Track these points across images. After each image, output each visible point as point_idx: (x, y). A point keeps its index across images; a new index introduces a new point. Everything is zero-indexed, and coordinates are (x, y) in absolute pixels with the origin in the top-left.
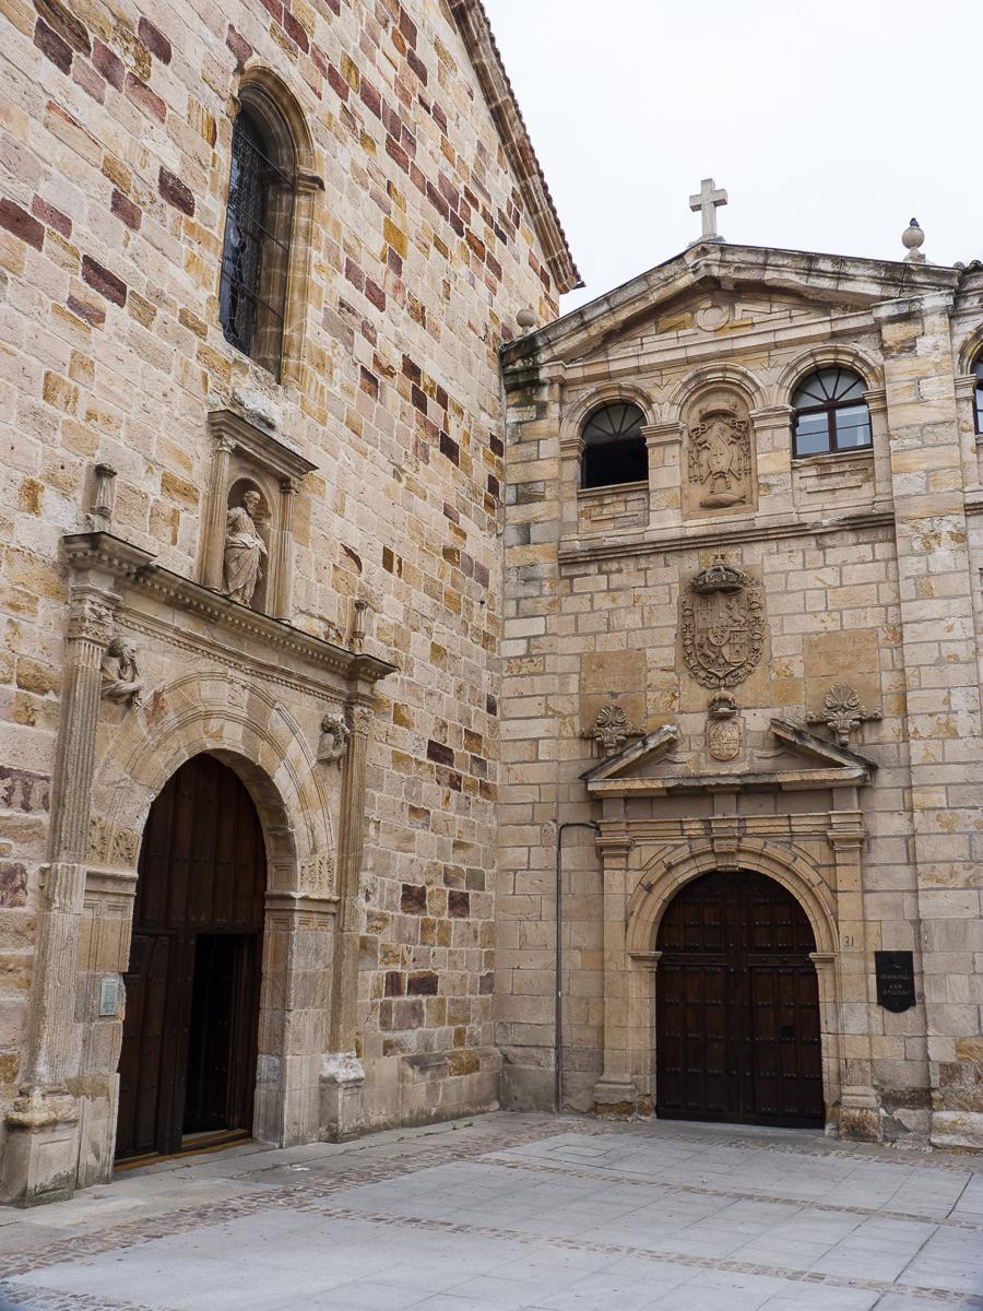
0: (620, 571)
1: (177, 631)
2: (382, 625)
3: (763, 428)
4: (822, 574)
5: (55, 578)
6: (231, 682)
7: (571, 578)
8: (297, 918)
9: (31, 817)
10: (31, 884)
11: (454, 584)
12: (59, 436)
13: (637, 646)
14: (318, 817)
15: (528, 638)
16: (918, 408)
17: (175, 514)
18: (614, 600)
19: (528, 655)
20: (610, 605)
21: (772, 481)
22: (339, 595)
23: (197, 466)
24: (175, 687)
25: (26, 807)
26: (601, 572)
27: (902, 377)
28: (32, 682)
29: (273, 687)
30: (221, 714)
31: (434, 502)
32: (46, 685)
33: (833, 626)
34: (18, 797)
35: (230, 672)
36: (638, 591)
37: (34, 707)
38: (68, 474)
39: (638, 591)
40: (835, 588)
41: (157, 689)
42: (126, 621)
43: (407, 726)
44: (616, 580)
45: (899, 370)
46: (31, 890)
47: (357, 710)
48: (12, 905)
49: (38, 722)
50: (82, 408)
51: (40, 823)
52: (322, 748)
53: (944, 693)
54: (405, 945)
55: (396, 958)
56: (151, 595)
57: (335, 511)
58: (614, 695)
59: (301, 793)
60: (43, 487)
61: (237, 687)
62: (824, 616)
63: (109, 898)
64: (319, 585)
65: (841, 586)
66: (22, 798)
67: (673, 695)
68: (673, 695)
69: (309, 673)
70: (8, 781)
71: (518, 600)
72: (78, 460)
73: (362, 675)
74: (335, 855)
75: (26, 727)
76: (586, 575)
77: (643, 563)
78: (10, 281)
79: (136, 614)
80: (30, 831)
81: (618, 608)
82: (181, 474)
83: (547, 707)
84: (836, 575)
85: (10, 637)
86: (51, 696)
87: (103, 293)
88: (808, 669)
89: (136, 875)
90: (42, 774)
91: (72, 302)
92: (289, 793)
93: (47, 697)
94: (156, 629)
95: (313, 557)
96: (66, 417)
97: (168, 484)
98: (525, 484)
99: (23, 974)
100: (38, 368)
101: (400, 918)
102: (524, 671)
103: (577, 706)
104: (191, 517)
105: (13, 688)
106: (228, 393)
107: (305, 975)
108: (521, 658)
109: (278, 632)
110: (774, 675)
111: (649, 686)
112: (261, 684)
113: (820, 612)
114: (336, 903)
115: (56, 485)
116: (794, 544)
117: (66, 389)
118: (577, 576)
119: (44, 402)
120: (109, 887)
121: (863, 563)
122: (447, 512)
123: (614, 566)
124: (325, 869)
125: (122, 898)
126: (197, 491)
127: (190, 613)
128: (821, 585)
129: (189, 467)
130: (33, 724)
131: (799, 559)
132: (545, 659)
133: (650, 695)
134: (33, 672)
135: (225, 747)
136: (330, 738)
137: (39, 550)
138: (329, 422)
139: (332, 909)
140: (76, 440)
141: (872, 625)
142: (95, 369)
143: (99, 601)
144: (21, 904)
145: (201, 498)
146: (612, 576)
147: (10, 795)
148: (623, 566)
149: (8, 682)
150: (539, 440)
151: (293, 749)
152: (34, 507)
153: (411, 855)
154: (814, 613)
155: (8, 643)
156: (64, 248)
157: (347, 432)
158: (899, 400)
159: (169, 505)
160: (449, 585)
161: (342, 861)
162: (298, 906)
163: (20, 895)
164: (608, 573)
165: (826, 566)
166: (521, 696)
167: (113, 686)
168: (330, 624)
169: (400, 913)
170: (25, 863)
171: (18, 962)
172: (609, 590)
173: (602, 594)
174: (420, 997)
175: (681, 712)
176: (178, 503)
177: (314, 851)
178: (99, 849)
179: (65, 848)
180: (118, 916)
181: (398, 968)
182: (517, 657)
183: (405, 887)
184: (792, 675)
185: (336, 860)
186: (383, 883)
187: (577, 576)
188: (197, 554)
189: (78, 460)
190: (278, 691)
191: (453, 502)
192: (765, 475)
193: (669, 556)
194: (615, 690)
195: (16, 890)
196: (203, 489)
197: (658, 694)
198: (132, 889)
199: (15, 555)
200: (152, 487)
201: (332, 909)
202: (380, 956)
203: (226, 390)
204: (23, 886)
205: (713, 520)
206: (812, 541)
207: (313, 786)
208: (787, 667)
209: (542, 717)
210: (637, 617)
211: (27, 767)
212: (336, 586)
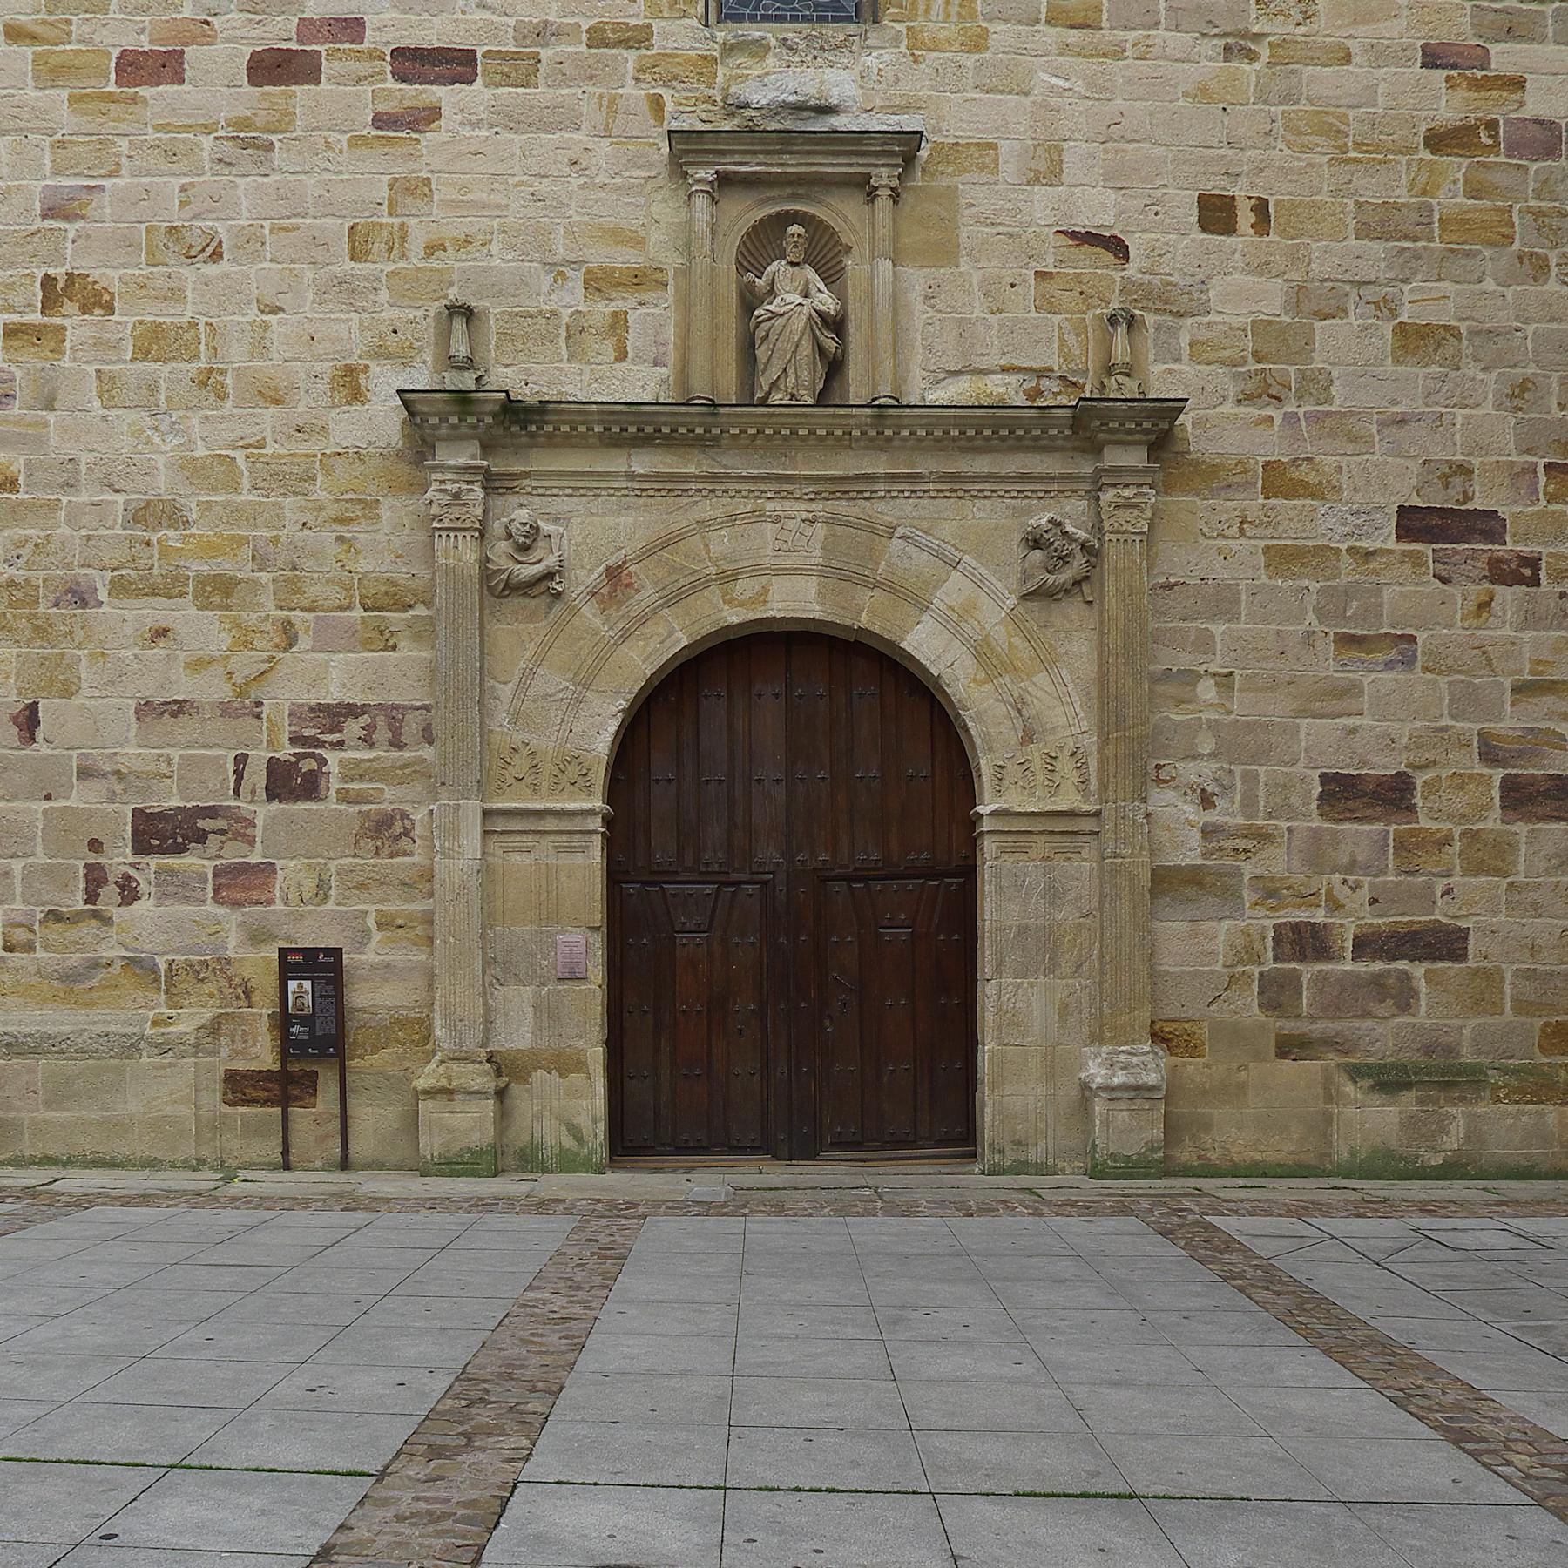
1: (631, 476)
2: (1203, 335)
5: (404, 469)
6: (778, 520)
8: (989, 846)
9: (406, 754)
10: (418, 831)
11: (1474, 192)
12: (384, 295)
14: (1040, 688)
17: (618, 323)
22: (1057, 319)
23: (655, 236)
24: (649, 552)
25: (397, 744)
28: (386, 600)
29: (879, 506)
30: (756, 571)
31: (1379, 54)
32: (410, 599)
34: (383, 734)
35: (770, 506)
37: (391, 629)
38: (406, 336)
41: (610, 563)
42: (536, 488)
43: (1313, 496)
46: (421, 838)
47: (1107, 496)
48: (392, 856)
49: (401, 645)
50: (416, 246)
51: (421, 760)
52: (1026, 577)
54: (1337, 877)
55: (1308, 899)
56: (556, 442)
57: (1035, 181)
59: (983, 653)
60: (367, 366)
61: (791, 524)
63: (551, 838)
64: (993, 319)
66: (390, 735)
69: (981, 464)
70: (365, 720)
72: (420, 313)
73: (1101, 436)
74: (1090, 741)
75: (385, 653)
78: (277, 144)
79: (527, 475)
80: (407, 771)
82: (625, 258)
85: (342, 556)
86: (420, 611)
87: (432, 83)
89: (597, 803)
90: (418, 704)
91: (379, 121)
92: (949, 659)
93: (412, 612)
94: (595, 484)
95: (976, 277)
96: (391, 267)
97: (597, 283)
99: (420, 930)
100: (335, 228)
101: (1316, 834)
104: (657, 311)
105: (358, 613)
106: (714, 103)
107: (1023, 930)
109: (851, 422)
112: (843, 506)
114: (1097, 814)
115: (389, 356)
117: (385, 234)
119: (353, 264)
120: (551, 824)
122: (1432, 58)
124: (1065, 766)
125: (577, 837)
126: (661, 270)
127: (659, 445)
129: (640, 243)
130: (394, 648)
134: (383, 589)
135: (771, 614)
136: (1037, 555)
137: (370, 443)
138: (993, 41)
139: (1087, 825)
140: (406, 288)
142: (433, 187)
143: (450, 476)
144: (410, 854)
145: (670, 277)
147: (370, 734)
149: (349, 607)
151: (954, 589)
152: (356, 395)
153: (1352, 721)
155: (340, 564)
156: (357, 59)
157: (1052, 35)
159: (602, 309)
160: (1461, 200)
161: (1100, 750)
162: (987, 826)
163: (404, 843)
167: (505, 576)
168: (1042, 373)
169: (1317, 823)
170: (407, 808)
171: (411, 916)
174: (1403, 965)
176: (623, 301)
177: (1028, 737)
178: (529, 780)
179: (443, 784)
180: (579, 859)
181: (1320, 917)
183: (1325, 779)
185: (1094, 748)
186: (1251, 779)
188: (672, 358)
189: (420, 313)
190: (884, 511)
191: (1461, 31)
195: (397, 838)
196: (672, 261)
198: (596, 824)
199: (337, 460)
200: (570, 299)
201: (1087, 825)
202: (1248, 896)
203: (709, 99)
204: (407, 833)
207: (1017, 641)
211: (393, 698)
212: (1047, 305)
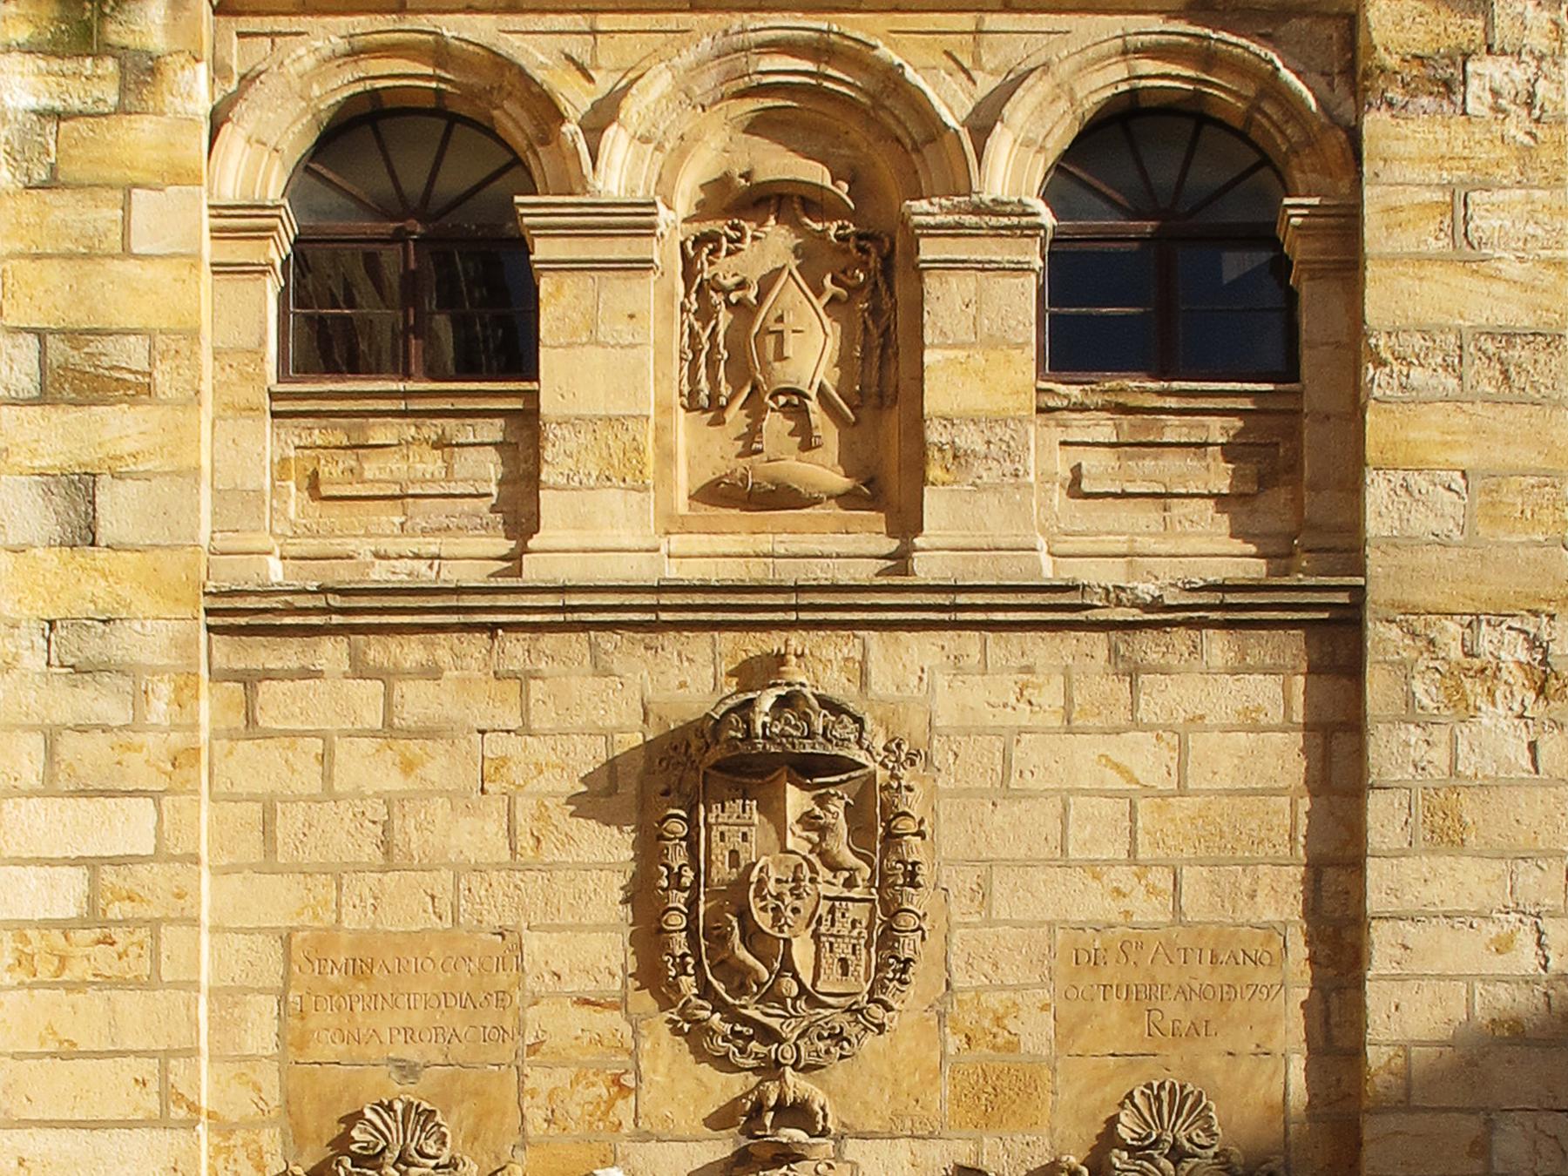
0: (432, 672)
3: (952, 265)
4: (1115, 748)
7: (249, 680)
13: (493, 920)
15: (92, 864)
16: (1462, 281)
18: (408, 767)
19: (93, 916)
20: (395, 782)
21: (970, 439)
26: (360, 670)
27: (1413, 174)
33: (1149, 910)
36: (496, 746)
39: (496, 746)
40: (1163, 795)
44: (417, 700)
45: (1412, 148)
53: (1472, 1126)
58: (407, 1070)
62: (1122, 876)
65: (1182, 791)
67: (616, 1081)
68: (616, 1081)
71: (51, 737)
76: (308, 674)
77: (515, 648)
81: (427, 794)
83: (169, 1095)
84: (1170, 757)
88: (1066, 1032)
98: (74, 335)
102: (72, 974)
103: (274, 1097)
108: (65, 927)
110: (954, 1042)
111: (533, 1049)
113: (1112, 863)
116: (1039, 647)
118: (269, 675)
121: (1256, 728)
123: (411, 651)
128: (1116, 782)
131: (1050, 696)
132: (156, 937)
133: (537, 1079)
141: (1269, 915)
146: (402, 688)
148: (443, 655)
150: (128, 188)
154: (1094, 868)
158: (1405, 241)
164: (387, 676)
165: (1136, 725)
166: (69, 1053)
172: (389, 730)
173: (365, 743)
175: (645, 1137)
182: (48, 924)
184: (1012, 1047)
187: (269, 675)
192: (948, 420)
193: (607, 640)
194: (411, 1054)
197: (562, 1076)
205: (765, 543)
206: (1098, 642)
208: (998, 1020)
209: (148, 1123)
210: (494, 828)
